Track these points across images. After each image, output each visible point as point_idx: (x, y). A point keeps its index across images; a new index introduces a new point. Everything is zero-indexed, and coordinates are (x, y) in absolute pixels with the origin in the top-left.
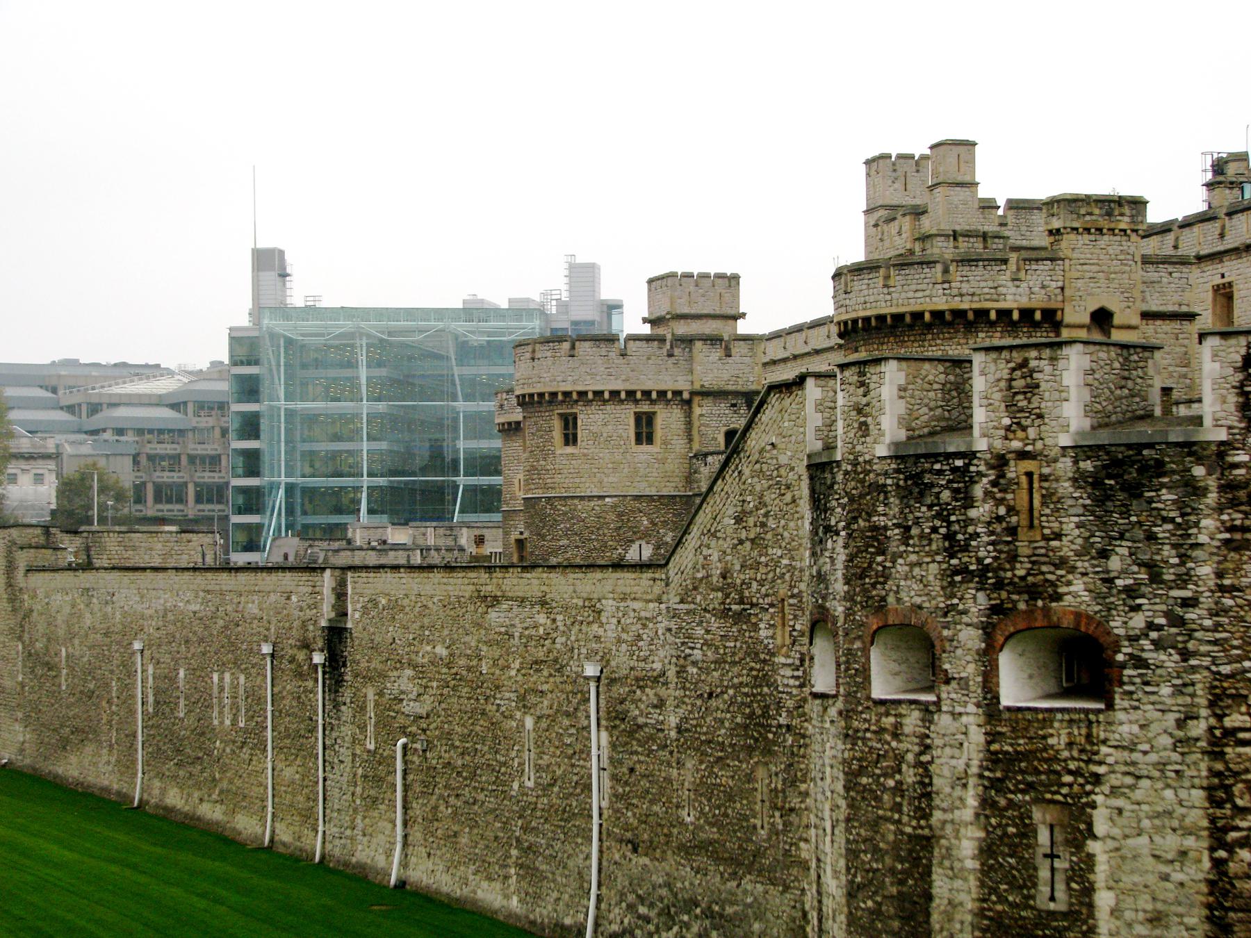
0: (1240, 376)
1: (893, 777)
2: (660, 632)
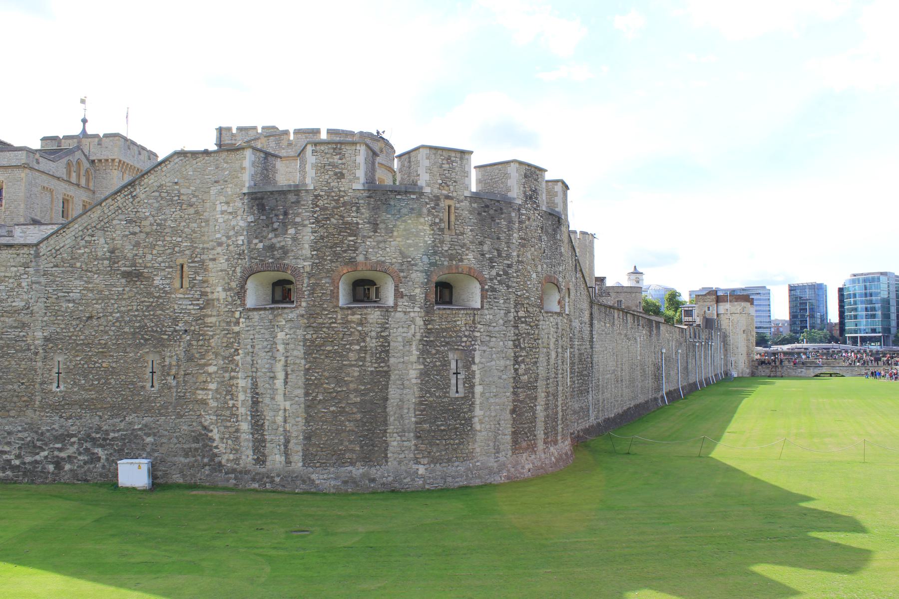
0: (524, 180)
1: (358, 344)
2: (24, 284)
